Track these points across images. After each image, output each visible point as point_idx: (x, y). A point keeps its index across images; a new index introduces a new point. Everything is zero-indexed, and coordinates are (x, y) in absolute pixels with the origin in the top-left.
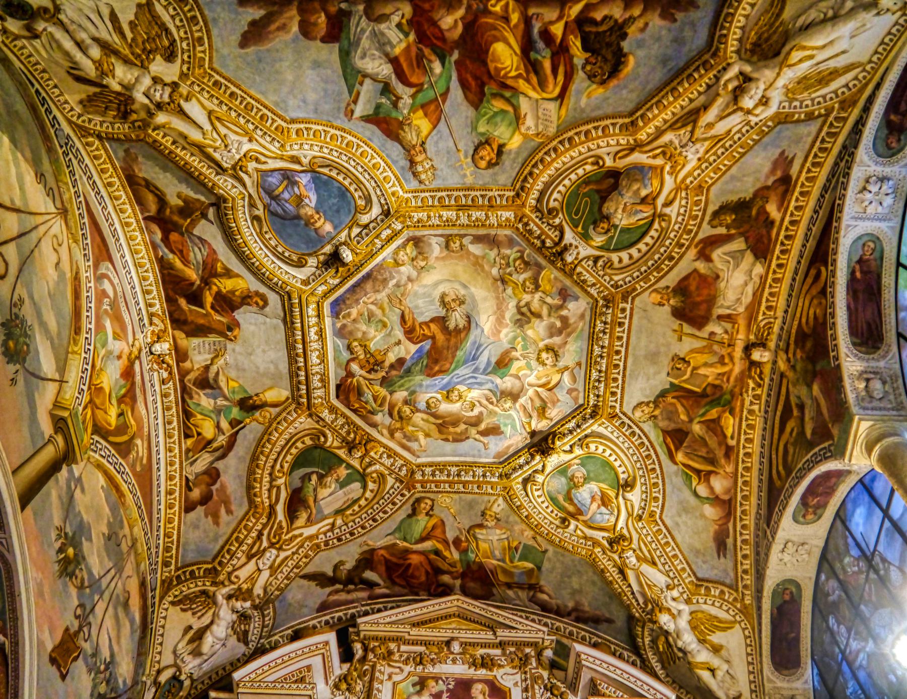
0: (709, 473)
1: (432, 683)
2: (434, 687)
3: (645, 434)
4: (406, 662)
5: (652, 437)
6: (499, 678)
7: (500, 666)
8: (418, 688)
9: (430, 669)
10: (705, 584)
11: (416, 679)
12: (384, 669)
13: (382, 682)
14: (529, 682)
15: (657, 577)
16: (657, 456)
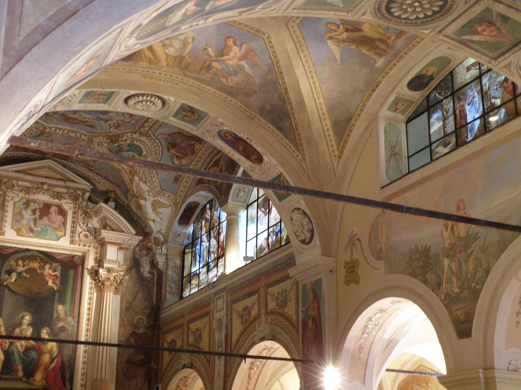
0: (181, 158)
1: (32, 204)
2: (33, 206)
3: (160, 143)
4: (21, 191)
5: (163, 144)
6: (63, 205)
7: (65, 199)
8: (25, 206)
9: (32, 197)
10: (164, 192)
11: (25, 201)
12: (10, 194)
13: (8, 202)
14: (77, 209)
15: (145, 187)
16: (162, 149)
